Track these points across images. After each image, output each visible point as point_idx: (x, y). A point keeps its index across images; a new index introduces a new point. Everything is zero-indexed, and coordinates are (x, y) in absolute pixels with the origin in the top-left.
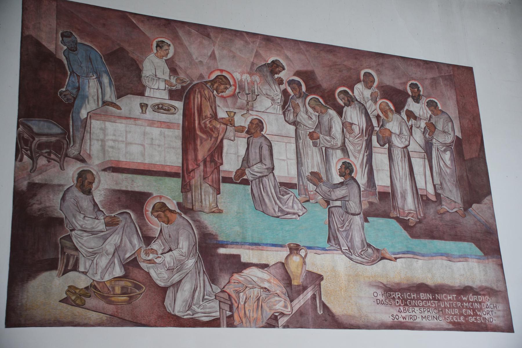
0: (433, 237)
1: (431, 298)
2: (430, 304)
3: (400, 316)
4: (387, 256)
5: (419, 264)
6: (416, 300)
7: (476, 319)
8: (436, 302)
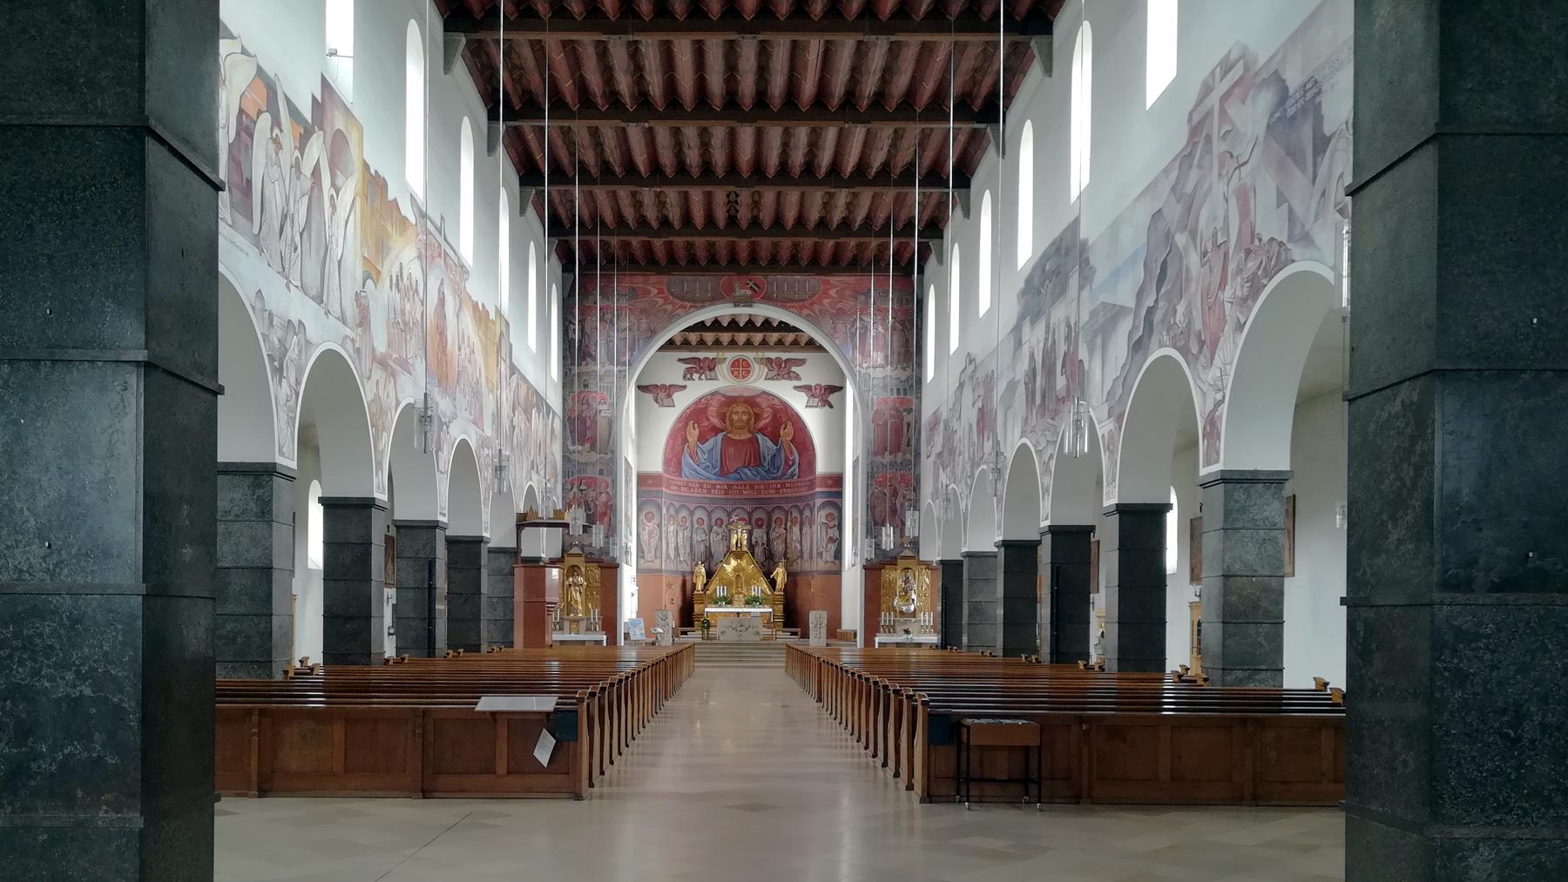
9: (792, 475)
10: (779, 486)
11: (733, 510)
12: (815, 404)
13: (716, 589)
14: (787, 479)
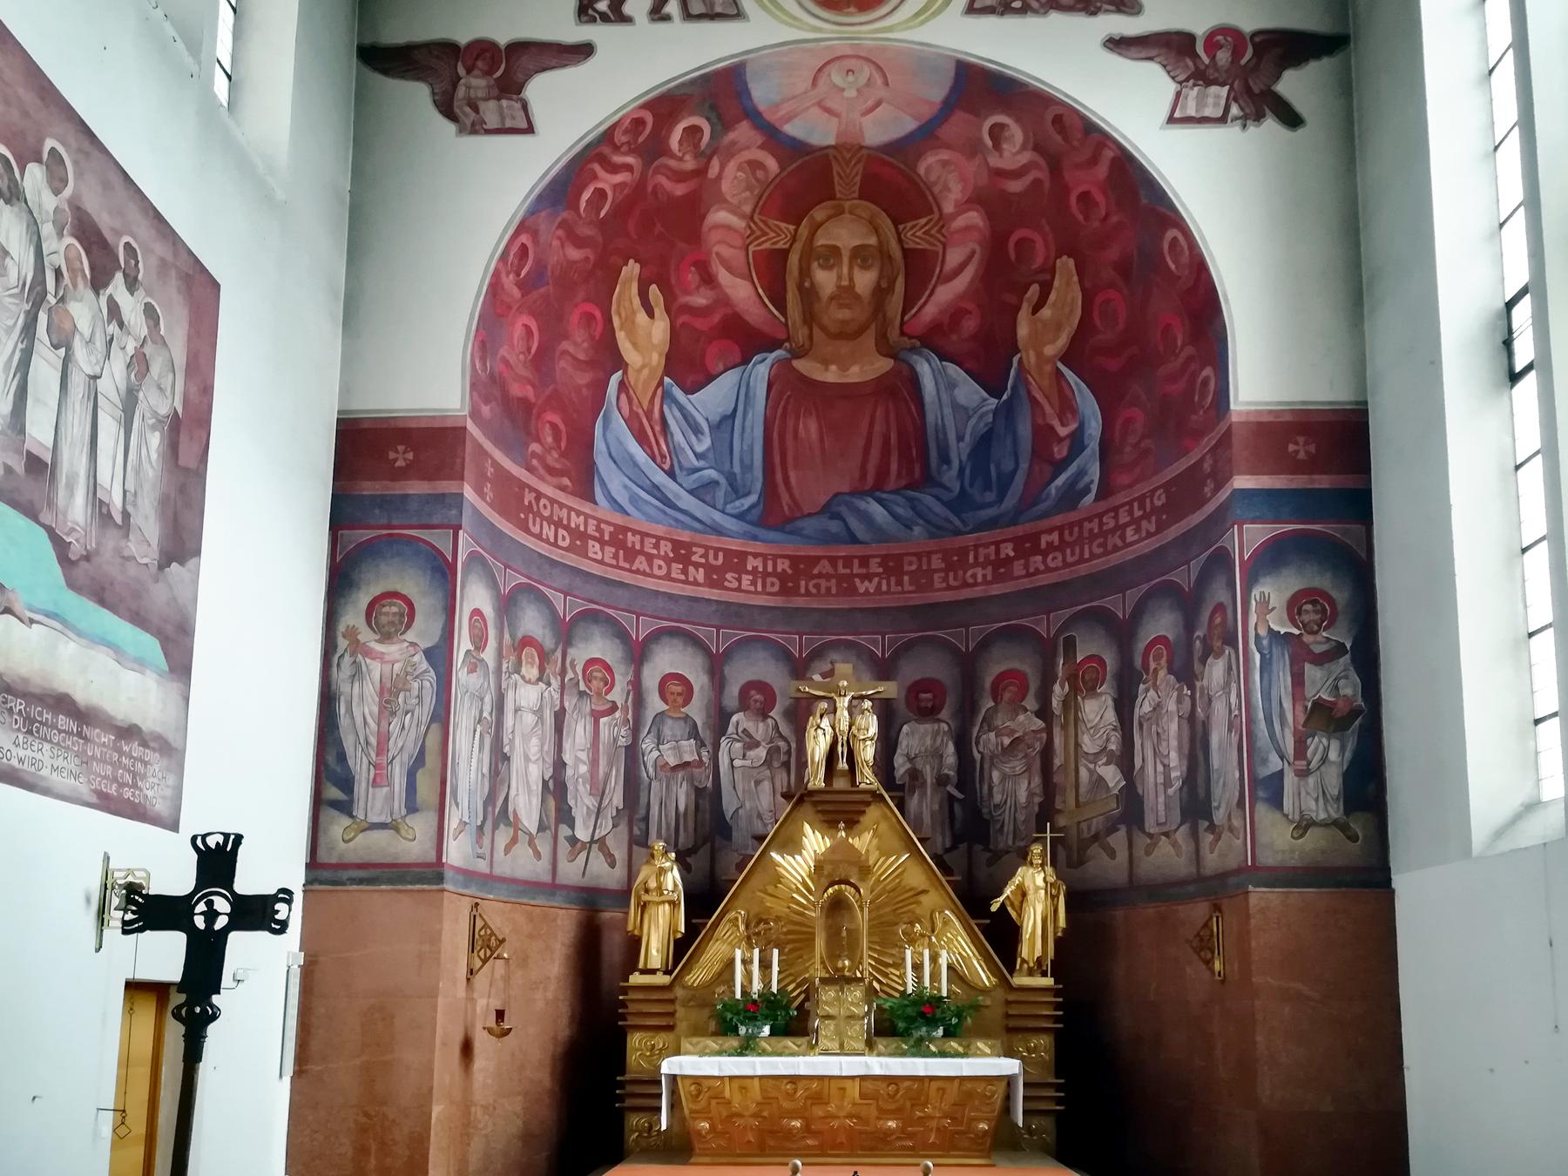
0: (102, 603)
1: (75, 730)
2: (70, 743)
3: (14, 754)
4: (17, 608)
5: (69, 648)
6: (51, 727)
7: (133, 795)
8: (82, 741)
9: (1072, 495)
10: (1008, 550)
11: (818, 654)
12: (1208, 112)
13: (730, 964)
14: (1046, 515)
